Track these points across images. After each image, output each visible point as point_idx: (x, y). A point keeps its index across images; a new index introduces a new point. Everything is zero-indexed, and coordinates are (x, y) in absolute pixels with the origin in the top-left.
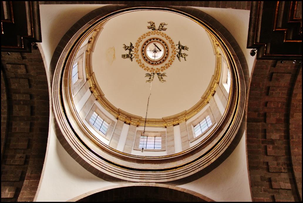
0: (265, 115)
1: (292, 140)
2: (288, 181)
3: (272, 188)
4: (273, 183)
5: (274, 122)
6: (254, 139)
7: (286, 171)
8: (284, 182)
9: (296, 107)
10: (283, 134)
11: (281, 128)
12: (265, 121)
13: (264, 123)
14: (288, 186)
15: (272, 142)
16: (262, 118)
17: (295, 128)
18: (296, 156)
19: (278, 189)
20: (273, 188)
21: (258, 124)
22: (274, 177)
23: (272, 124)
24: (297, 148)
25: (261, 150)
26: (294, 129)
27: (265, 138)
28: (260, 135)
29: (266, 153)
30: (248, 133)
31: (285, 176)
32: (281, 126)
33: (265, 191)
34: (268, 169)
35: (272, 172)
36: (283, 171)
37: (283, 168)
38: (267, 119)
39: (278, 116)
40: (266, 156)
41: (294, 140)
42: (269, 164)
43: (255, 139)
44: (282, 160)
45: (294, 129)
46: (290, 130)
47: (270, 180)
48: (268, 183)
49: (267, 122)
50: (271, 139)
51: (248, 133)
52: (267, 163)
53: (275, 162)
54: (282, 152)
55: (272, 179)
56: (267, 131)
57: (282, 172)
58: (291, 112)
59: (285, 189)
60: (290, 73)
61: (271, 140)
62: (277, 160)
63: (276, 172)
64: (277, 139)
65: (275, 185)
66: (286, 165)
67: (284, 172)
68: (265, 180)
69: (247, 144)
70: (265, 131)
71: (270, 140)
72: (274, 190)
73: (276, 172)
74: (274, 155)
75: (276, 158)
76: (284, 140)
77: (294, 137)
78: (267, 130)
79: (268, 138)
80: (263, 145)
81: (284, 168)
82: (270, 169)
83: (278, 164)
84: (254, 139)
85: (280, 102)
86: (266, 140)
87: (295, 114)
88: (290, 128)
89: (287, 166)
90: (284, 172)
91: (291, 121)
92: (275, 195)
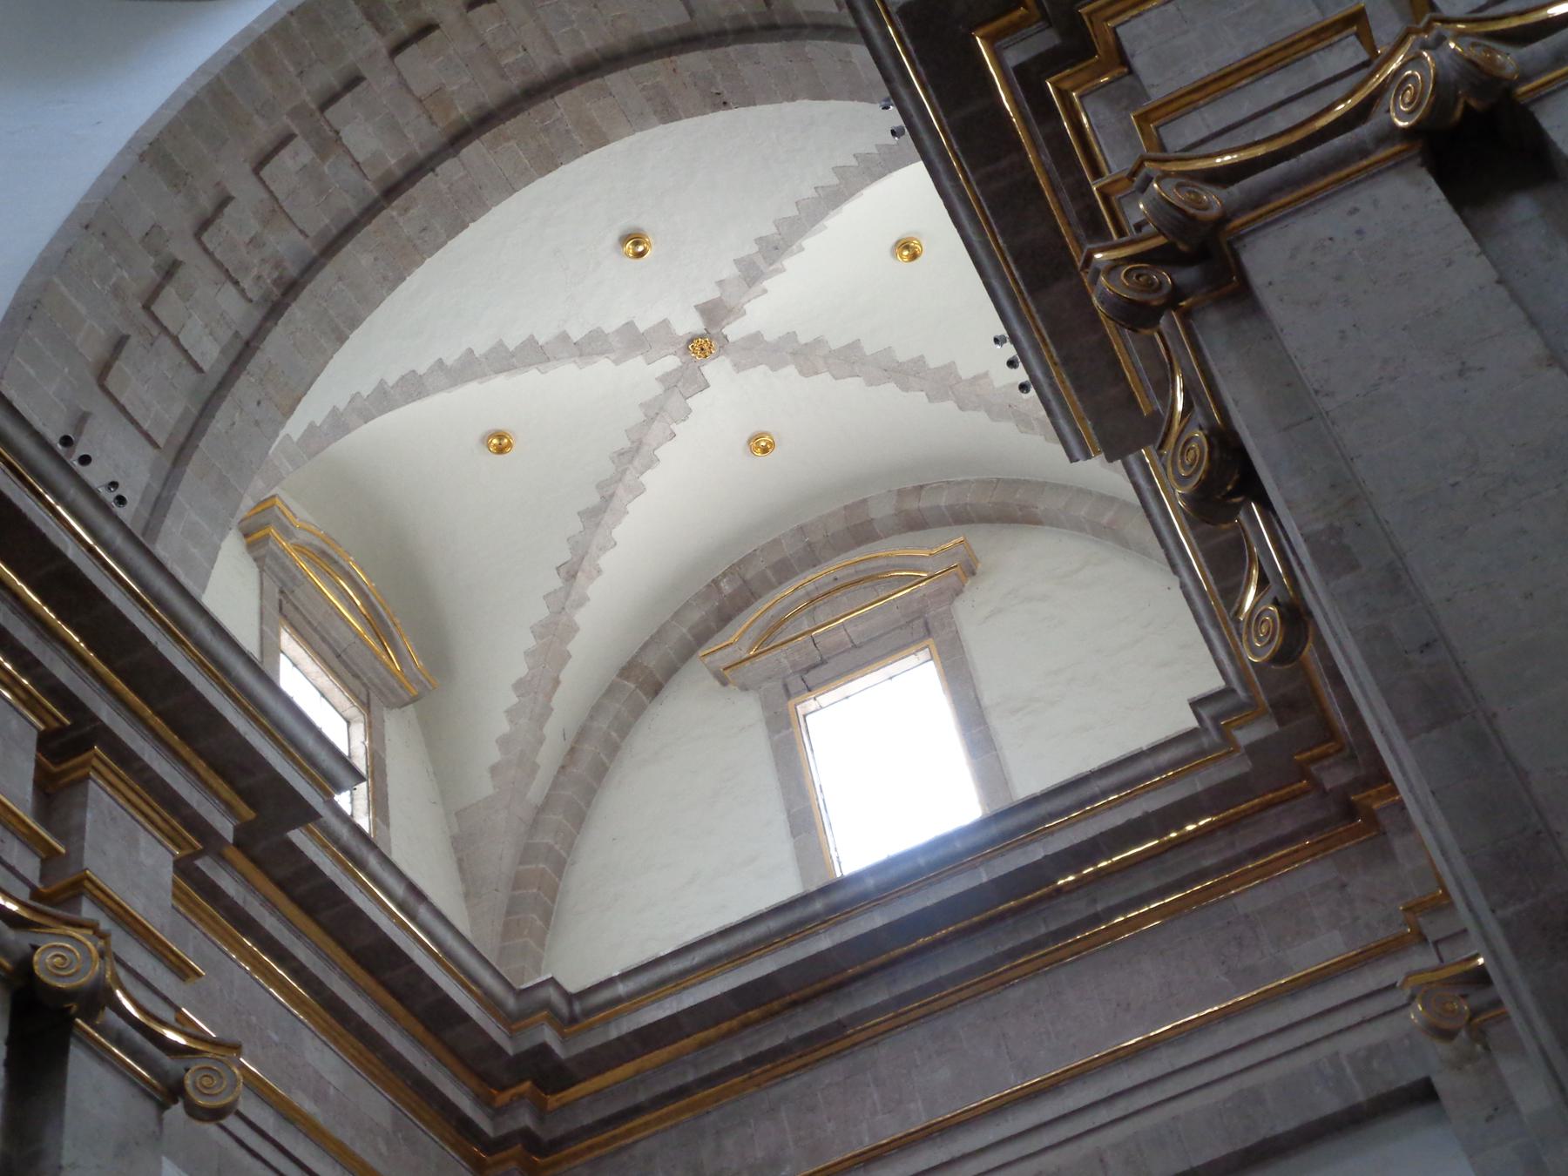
0: (426, 29)
1: (394, 213)
2: (225, 335)
3: (147, 307)
4: (170, 292)
5: (419, 90)
6: (286, 62)
7: (254, 294)
8: (206, 326)
9: (546, 130)
10: (393, 162)
11: (411, 136)
12: (397, 49)
13: (384, 52)
14: (210, 353)
15: (329, 143)
16: (404, 28)
17: (452, 184)
18: (340, 279)
19: (165, 329)
20: (153, 308)
21: (367, 30)
22: (196, 270)
23: (404, 84)
24: (376, 259)
25: (263, 133)
26: (443, 187)
27: (323, 107)
28: (326, 76)
29: (262, 162)
30: (294, 22)
31: (235, 309)
32: (421, 135)
33: (117, 291)
34: (204, 225)
35: (206, 250)
36: (246, 283)
37: (258, 277)
38: (413, 51)
39: (455, 88)
40: (248, 168)
41: (401, 220)
42: (228, 210)
43: (291, 69)
44: (287, 245)
45: (443, 187)
46: (430, 175)
47: (170, 270)
48: (152, 271)
49: (401, 59)
50: (337, 132)
51: (294, 22)
52: (225, 201)
53: (254, 226)
54: (319, 219)
55: (181, 273)
56: (358, 89)
57: (236, 283)
58: (511, 126)
59: (185, 352)
60: (691, 13)
61: (331, 134)
62: (265, 223)
63: (219, 264)
64: (356, 155)
65: (168, 307)
66: (276, 275)
67: (242, 292)
68: (156, 253)
69: (237, 51)
70: (353, 81)
71: (327, 128)
72: (143, 317)
73: (219, 264)
74: (281, 197)
75: (275, 210)
76: (369, 185)
77: (413, 212)
78: (364, 84)
79: (330, 113)
80: (286, 122)
81: (259, 277)
82: (212, 230)
83: (255, 242)
84: (286, 62)
85: (525, 50)
86: (318, 114)
87: (512, 143)
88: (438, 170)
89: (275, 282)
90: (242, 292)
91: (474, 151)
92: (133, 341)
